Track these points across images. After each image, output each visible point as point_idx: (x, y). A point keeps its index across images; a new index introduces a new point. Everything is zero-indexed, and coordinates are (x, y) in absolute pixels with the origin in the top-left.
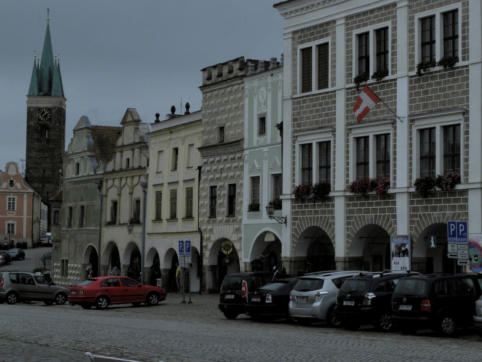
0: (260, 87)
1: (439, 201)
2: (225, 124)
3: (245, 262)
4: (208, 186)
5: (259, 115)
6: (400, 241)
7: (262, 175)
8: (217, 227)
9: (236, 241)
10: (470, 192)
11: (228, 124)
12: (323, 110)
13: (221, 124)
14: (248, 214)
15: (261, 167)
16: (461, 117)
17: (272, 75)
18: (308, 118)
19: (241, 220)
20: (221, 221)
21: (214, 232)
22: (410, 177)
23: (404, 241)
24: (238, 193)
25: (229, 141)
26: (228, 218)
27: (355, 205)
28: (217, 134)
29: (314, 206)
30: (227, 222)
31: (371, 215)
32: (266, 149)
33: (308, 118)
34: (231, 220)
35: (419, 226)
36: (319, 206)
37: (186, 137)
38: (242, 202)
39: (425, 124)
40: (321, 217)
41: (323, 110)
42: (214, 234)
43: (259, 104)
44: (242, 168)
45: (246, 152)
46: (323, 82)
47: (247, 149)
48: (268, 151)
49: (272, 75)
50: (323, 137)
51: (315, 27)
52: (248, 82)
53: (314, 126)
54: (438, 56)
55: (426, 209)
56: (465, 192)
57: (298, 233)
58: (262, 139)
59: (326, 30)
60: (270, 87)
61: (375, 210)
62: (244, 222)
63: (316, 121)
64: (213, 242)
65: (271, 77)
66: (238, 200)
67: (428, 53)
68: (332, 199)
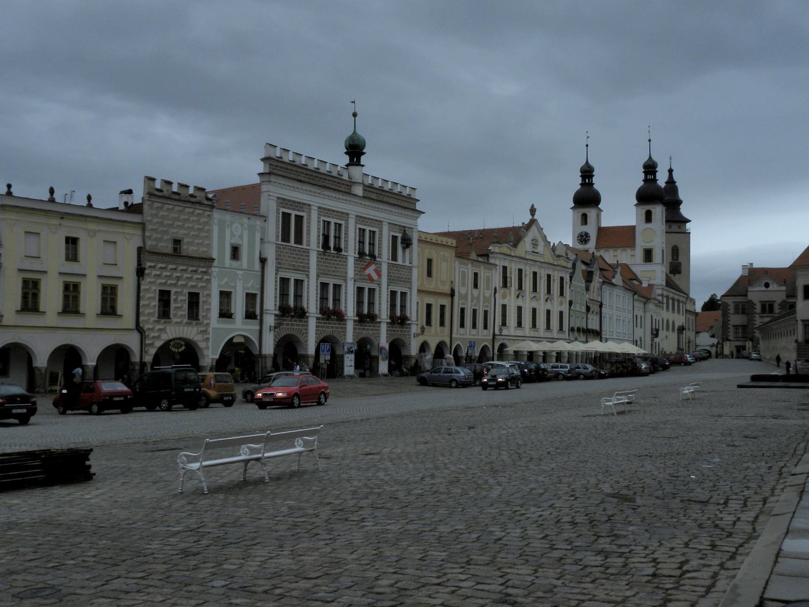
1: (366, 326)
2: (183, 239)
4: (156, 289)
5: (231, 244)
6: (349, 346)
7: (236, 291)
8: (172, 327)
9: (201, 341)
10: (382, 323)
11: (186, 240)
12: (300, 259)
13: (178, 237)
16: (408, 289)
17: (249, 218)
18: (287, 260)
19: (208, 324)
20: (177, 323)
21: (168, 332)
22: (275, 305)
23: (352, 346)
24: (203, 302)
25: (189, 255)
27: (321, 323)
29: (291, 321)
30: (188, 324)
31: (330, 330)
33: (287, 260)
35: (279, 334)
36: (295, 321)
37: (99, 231)
38: (209, 310)
39: (325, 280)
40: (296, 329)
41: (300, 259)
43: (233, 236)
44: (209, 281)
45: (213, 269)
46: (299, 240)
47: (216, 267)
49: (249, 218)
50: (299, 277)
51: (294, 202)
53: (292, 267)
54: (367, 251)
55: (360, 329)
56: (380, 322)
57: (277, 338)
58: (235, 264)
59: (302, 208)
60: (246, 226)
61: (332, 327)
63: (293, 265)
67: (337, 242)
68: (345, 320)
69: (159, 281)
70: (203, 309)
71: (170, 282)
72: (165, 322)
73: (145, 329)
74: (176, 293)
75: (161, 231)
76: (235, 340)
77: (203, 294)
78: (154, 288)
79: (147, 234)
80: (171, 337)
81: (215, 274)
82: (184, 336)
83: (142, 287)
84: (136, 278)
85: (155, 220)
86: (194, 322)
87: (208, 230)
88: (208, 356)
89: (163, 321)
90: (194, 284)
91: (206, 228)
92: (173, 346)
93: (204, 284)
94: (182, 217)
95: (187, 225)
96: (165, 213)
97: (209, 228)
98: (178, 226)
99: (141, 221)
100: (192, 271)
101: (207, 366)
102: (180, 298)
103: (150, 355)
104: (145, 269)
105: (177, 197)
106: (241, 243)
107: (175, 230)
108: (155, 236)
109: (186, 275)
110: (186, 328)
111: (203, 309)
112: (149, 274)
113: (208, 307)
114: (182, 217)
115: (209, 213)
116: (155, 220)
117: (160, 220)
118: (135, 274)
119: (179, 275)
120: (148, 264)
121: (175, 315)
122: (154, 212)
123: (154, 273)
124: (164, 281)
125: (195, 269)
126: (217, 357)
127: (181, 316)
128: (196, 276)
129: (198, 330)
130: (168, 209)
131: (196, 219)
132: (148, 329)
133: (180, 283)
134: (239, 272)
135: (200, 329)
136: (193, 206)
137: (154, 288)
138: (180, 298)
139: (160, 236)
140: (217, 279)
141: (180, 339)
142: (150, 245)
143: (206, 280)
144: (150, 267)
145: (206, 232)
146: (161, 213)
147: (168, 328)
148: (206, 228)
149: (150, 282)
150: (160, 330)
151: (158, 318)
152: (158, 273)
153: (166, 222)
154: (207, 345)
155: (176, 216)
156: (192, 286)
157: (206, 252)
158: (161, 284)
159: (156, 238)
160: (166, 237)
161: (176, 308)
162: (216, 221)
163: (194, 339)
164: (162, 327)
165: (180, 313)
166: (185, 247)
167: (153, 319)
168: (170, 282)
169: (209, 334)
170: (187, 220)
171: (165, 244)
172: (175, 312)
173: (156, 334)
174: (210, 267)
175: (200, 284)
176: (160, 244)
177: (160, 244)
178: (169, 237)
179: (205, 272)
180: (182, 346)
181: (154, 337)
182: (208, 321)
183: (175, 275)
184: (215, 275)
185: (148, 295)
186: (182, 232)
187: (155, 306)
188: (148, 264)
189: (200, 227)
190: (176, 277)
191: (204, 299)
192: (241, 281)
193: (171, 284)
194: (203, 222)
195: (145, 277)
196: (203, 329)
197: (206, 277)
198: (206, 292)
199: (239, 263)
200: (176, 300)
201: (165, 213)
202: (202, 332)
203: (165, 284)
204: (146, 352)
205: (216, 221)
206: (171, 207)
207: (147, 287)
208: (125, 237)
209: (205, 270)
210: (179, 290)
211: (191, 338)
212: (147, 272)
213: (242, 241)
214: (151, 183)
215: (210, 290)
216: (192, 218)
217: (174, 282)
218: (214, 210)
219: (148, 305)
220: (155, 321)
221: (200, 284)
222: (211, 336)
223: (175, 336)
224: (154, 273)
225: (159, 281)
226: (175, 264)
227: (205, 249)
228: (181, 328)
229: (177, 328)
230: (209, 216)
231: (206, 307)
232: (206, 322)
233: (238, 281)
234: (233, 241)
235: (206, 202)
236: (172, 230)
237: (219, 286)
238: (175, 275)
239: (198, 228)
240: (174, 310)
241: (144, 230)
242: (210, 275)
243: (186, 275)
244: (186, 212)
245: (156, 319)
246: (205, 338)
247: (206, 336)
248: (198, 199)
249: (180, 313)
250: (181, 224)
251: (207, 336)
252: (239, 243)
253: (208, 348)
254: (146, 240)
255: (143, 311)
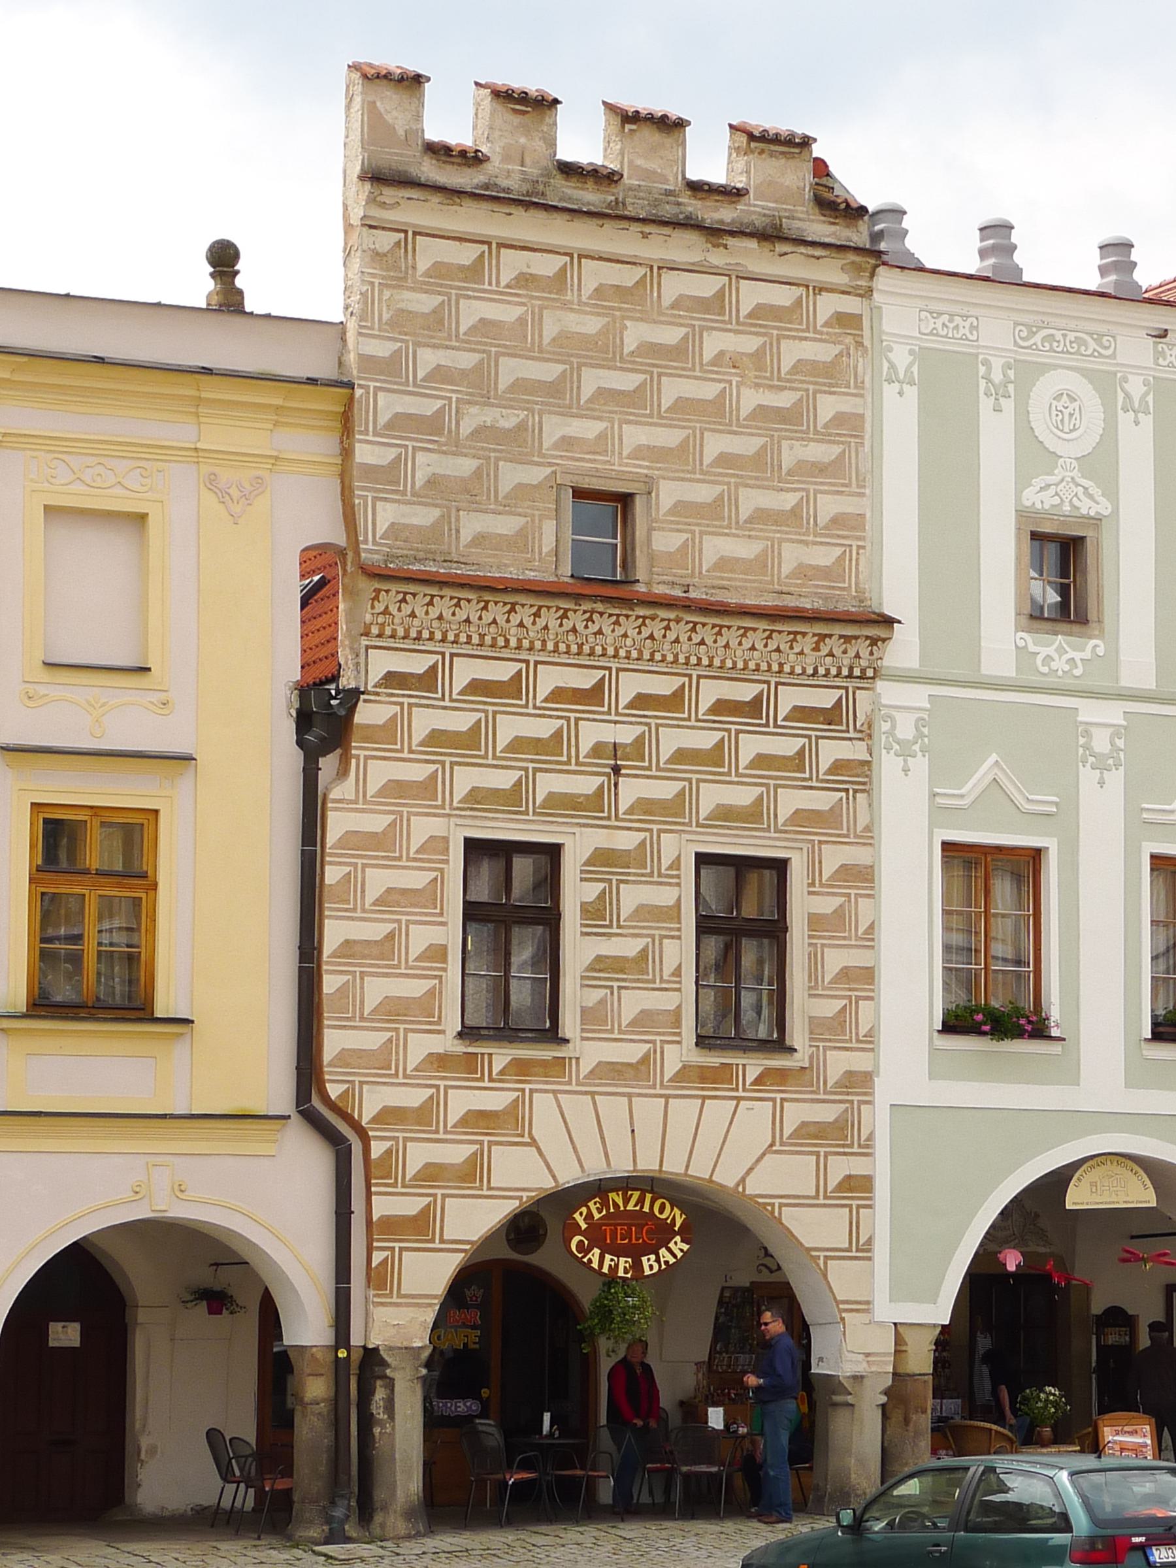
0: (1044, 368)
3: (895, 1324)
5: (1023, 514)
7: (1071, 848)
8: (578, 1107)
11: (668, 494)
14: (933, 1051)
15: (1056, 804)
24: (815, 922)
26: (714, 1059)
28: (549, 527)
32: (1113, 713)
34: (752, 1074)
42: (533, 1143)
48: (1125, 728)
52: (921, 304)
60: (1136, 387)
62: (885, 1093)
64: (525, 1195)
65: (1151, 340)
66: (815, 961)
69: (466, 779)
70: (814, 974)
71: (548, 784)
72: (521, 1068)
73: (367, 1111)
74: (603, 858)
75: (479, 432)
76: (1077, 1198)
77: (815, 865)
78: (423, 828)
79: (365, 454)
80: (569, 1176)
81: (905, 729)
82: (674, 1166)
83: (337, 825)
84: (291, 757)
85: (428, 359)
86: (753, 1066)
87: (840, 419)
88: (864, 1306)
89: (501, 1056)
90: (743, 796)
91: (828, 407)
92: (597, 1236)
93: (822, 801)
94: (635, 334)
95: (673, 389)
96: (506, 313)
97: (846, 405)
98: (604, 394)
99: (325, 371)
100: (722, 707)
101: (858, 1379)
102: (631, 897)
103: (415, 1301)
104: (353, 696)
105: (590, 196)
106: (1103, 507)
107: (588, 429)
108: (426, 465)
109: (672, 740)
110: (684, 1110)
111: (814, 974)
112: (388, 732)
113: (856, 958)
114: (635, 334)
115: (851, 305)
116: (428, 359)
117: (466, 360)
118: (288, 728)
119: (625, 735)
120: (381, 663)
121: (591, 1017)
122: (424, 303)
123: (425, 721)
124: (504, 780)
125: (745, 692)
126: (941, 1312)
127: (645, 1020)
128: (751, 746)
129: (777, 1120)
130: (525, 280)
131: (749, 344)
132: (389, 1116)
133: (631, 790)
134: (1089, 711)
135: (796, 1114)
136: (717, 258)
137: (423, 828)
138: (631, 897)
139: (464, 466)
140: (920, 765)
141: (651, 1185)
142: (394, 530)
143: (838, 767)
144: (393, 680)
145: (825, 437)
146: (472, 312)
147: (543, 1108)
148: (828, 407)
149: (397, 789)
150: (478, 1120)
151: (468, 1033)
152: (460, 722)
153: (510, 370)
154: (854, 1227)
155: (591, 325)
156: (726, 814)
157: (825, 572)
158: (478, 798)
159: (433, 482)
160: (511, 476)
161: (601, 964)
162: (901, 357)
163: (753, 1187)
164: (496, 1100)
165: (633, 1002)
166: (665, 541)
167: (420, 1046)
168: (548, 784)
169: (867, 1149)
170: (678, 352)
171: (506, 525)
172: (595, 995)
173: (456, 1154)
174: (868, 676)
175: (790, 801)
176: (471, 525)
177: (471, 525)
178: (536, 475)
179: (831, 716)
180: (662, 1234)
181: (432, 1174)
182: (859, 1062)
183: (592, 733)
184: (905, 729)
185: (378, 881)
186: (636, 435)
187: (438, 953)
188: (381, 663)
189: (784, 400)
190: (598, 750)
191: (826, 905)
192: (1116, 778)
193: (561, 804)
194: (800, 366)
195: (359, 748)
196: (827, 1113)
197: (831, 751)
198: (833, 858)
199: (1094, 646)
200: (595, 912)
201: (506, 313)
202: (811, 1133)
203: (512, 799)
204: (379, 1278)
205: (901, 357)
206: (547, 265)
207: (376, 823)
208: (211, 482)
209: (825, 699)
210: (626, 841)
211: (726, 1177)
212: (366, 714)
213: (1112, 494)
214: (389, 102)
215: (868, 837)
216: (714, 343)
217: (586, 785)
218: (885, 279)
219: (386, 948)
220: (440, 1061)
221: (790, 801)
222: (881, 1168)
223: (596, 1168)
224: (425, 721)
225: (466, 779)
226: (582, 656)
227: (823, 557)
228: (649, 1109)
229: (613, 1108)
230: (846, 321)
231: (835, 961)
232: (838, 1063)
233: (1088, 776)
234: (1039, 499)
235: (821, 229)
236: (555, 428)
237: (939, 812)
238: (592, 733)
239: (761, 412)
240: (586, 982)
241: (346, 424)
242: (867, 734)
243: (672, 740)
244: (668, 298)
245: (447, 1042)
246: (833, 1181)
247: (839, 1168)
248: (754, 209)
249: (633, 1002)
250: (627, 381)
251: (857, 1166)
252: (1086, 507)
253: (861, 1250)
254: (362, 495)
255: (343, 990)
